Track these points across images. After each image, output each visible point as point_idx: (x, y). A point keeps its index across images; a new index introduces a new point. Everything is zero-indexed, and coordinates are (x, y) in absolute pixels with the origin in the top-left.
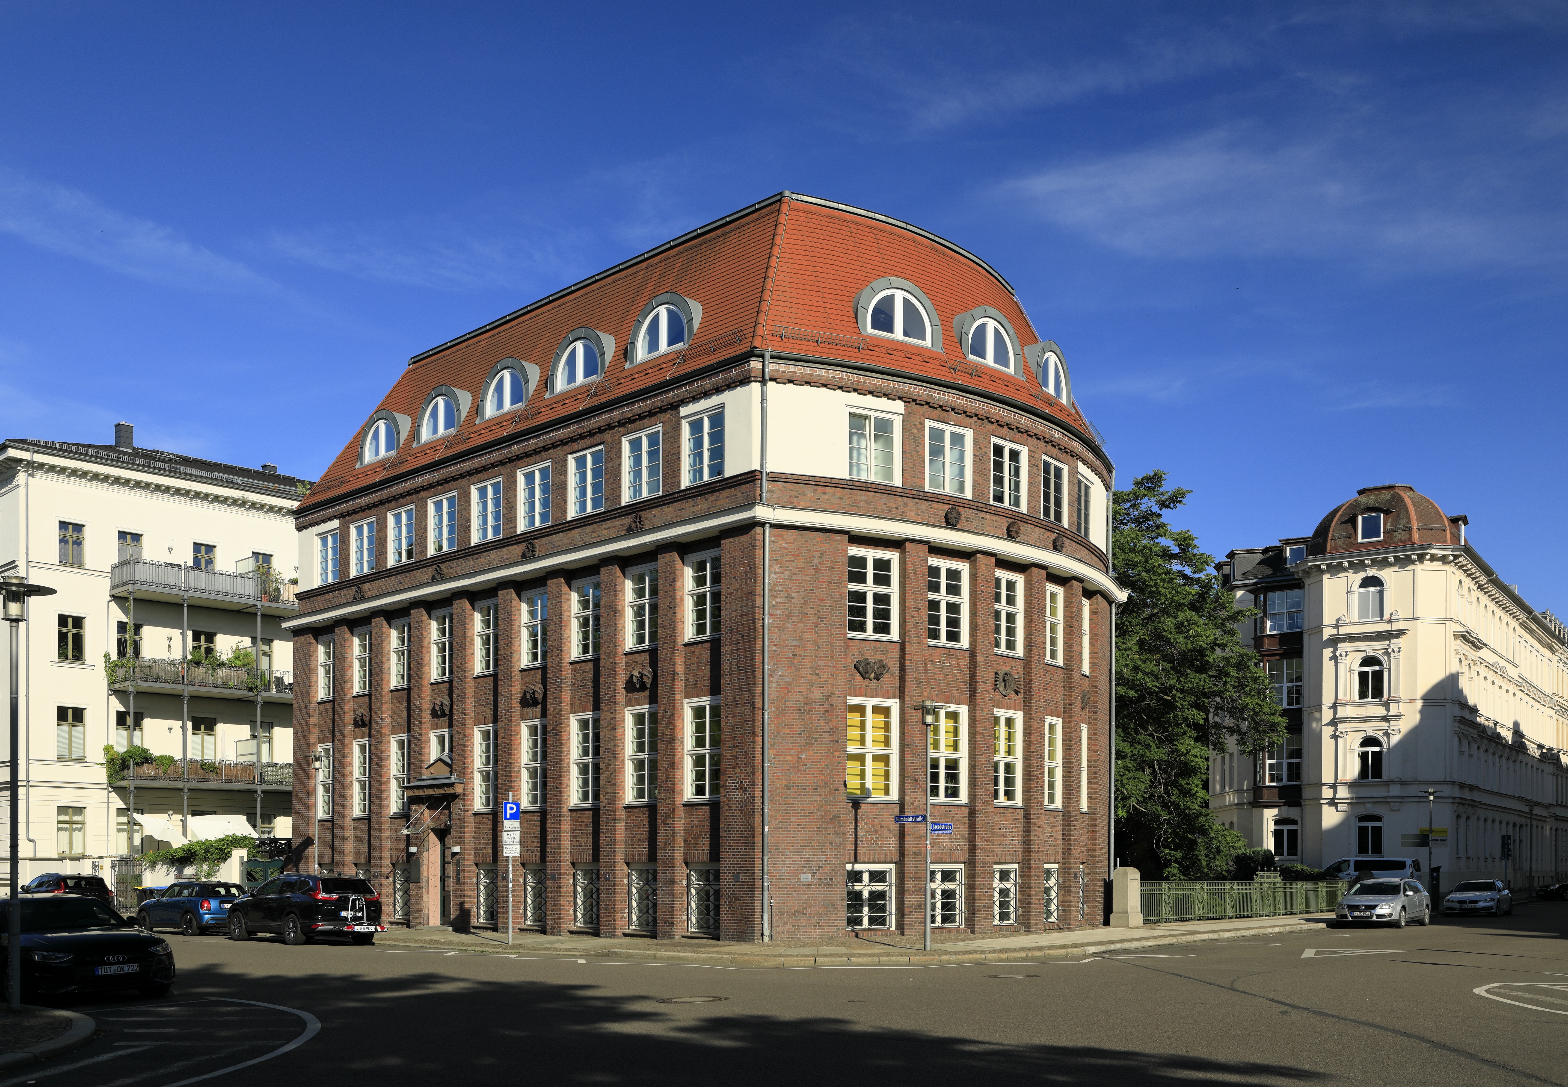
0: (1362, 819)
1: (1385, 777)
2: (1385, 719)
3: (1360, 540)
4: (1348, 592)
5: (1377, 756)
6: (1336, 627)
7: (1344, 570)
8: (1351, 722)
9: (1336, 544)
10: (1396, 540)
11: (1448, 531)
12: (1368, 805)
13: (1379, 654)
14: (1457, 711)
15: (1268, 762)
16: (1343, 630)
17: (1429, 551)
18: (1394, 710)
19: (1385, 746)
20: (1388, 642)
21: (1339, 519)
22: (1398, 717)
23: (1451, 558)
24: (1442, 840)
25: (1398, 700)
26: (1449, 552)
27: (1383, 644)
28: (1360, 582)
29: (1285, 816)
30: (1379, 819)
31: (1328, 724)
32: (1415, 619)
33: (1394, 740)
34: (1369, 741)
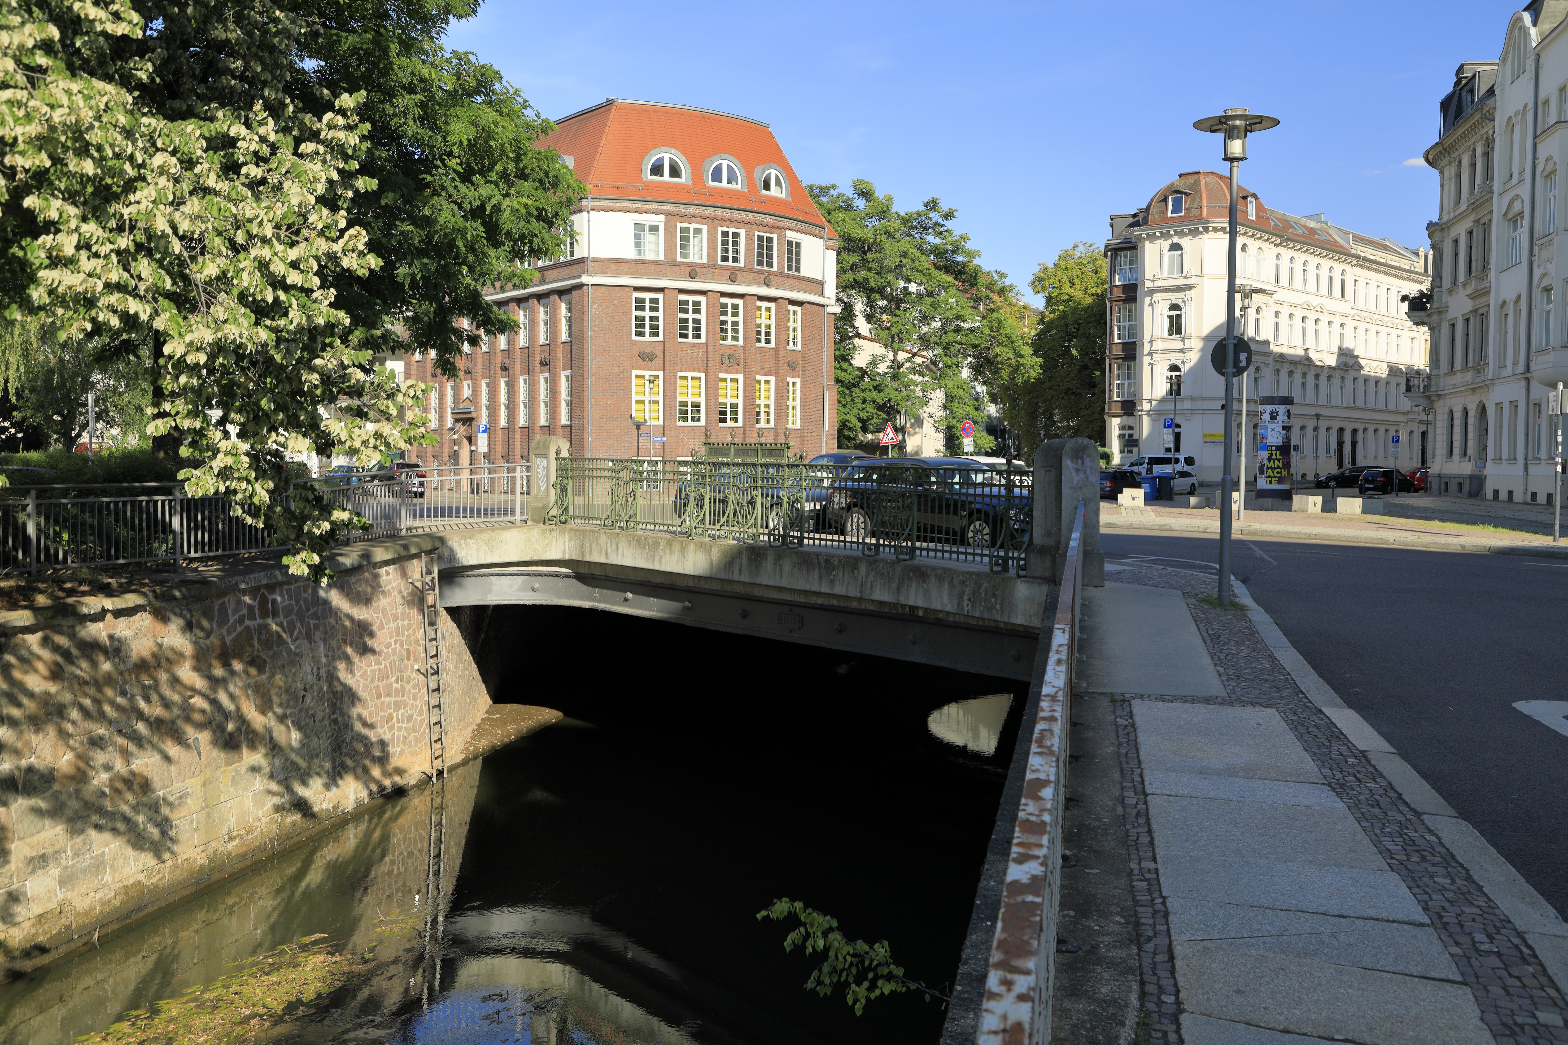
2: (1182, 351)
3: (1170, 215)
6: (1153, 281)
7: (1158, 238)
13: (1179, 302)
15: (1117, 382)
16: (1158, 284)
22: (1190, 349)
25: (1190, 337)
27: (1181, 295)
29: (1125, 423)
32: (1202, 275)
33: (1188, 367)
34: (1174, 368)
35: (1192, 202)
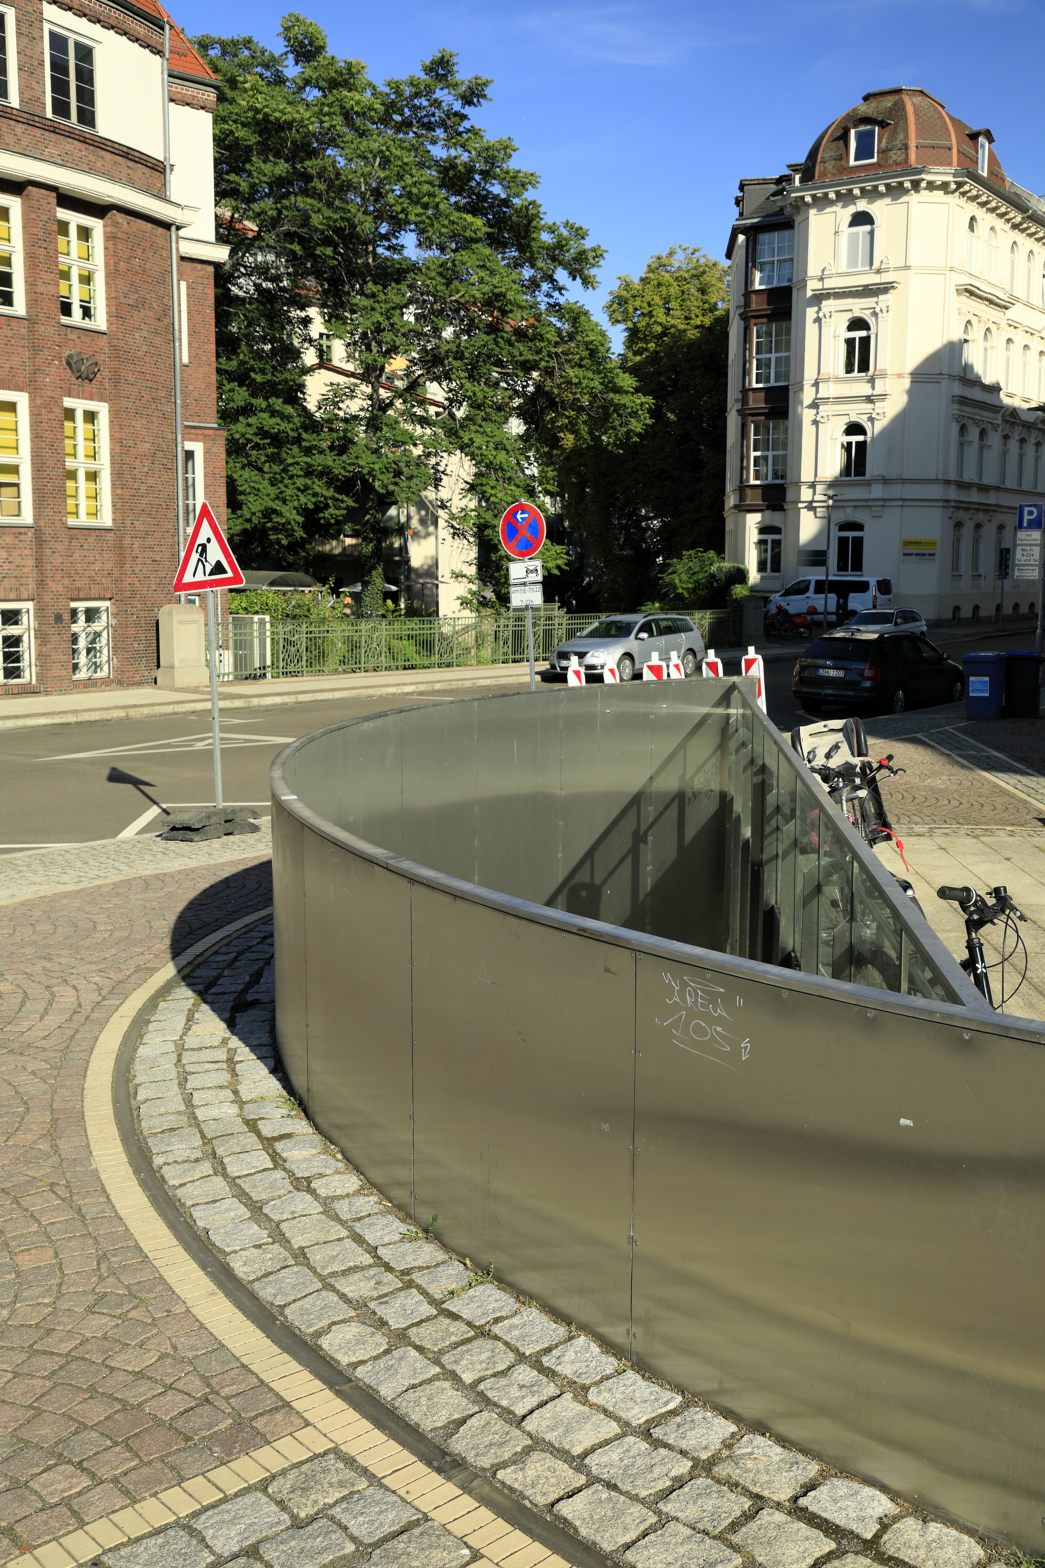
0: (843, 527)
1: (868, 476)
2: (869, 399)
3: (852, 162)
4: (836, 233)
5: (861, 446)
6: (821, 279)
7: (832, 203)
8: (833, 403)
9: (825, 168)
10: (890, 161)
11: (955, 150)
12: (849, 510)
13: (866, 315)
14: (957, 389)
15: (753, 454)
16: (829, 283)
17: (923, 176)
18: (880, 387)
19: (869, 434)
20: (875, 299)
21: (832, 134)
22: (883, 396)
23: (953, 186)
24: (930, 555)
25: (884, 375)
26: (950, 178)
27: (869, 302)
28: (850, 219)
29: (768, 523)
30: (859, 527)
31: (809, 407)
32: (907, 268)
33: (879, 426)
34: (854, 428)
35: (892, 138)
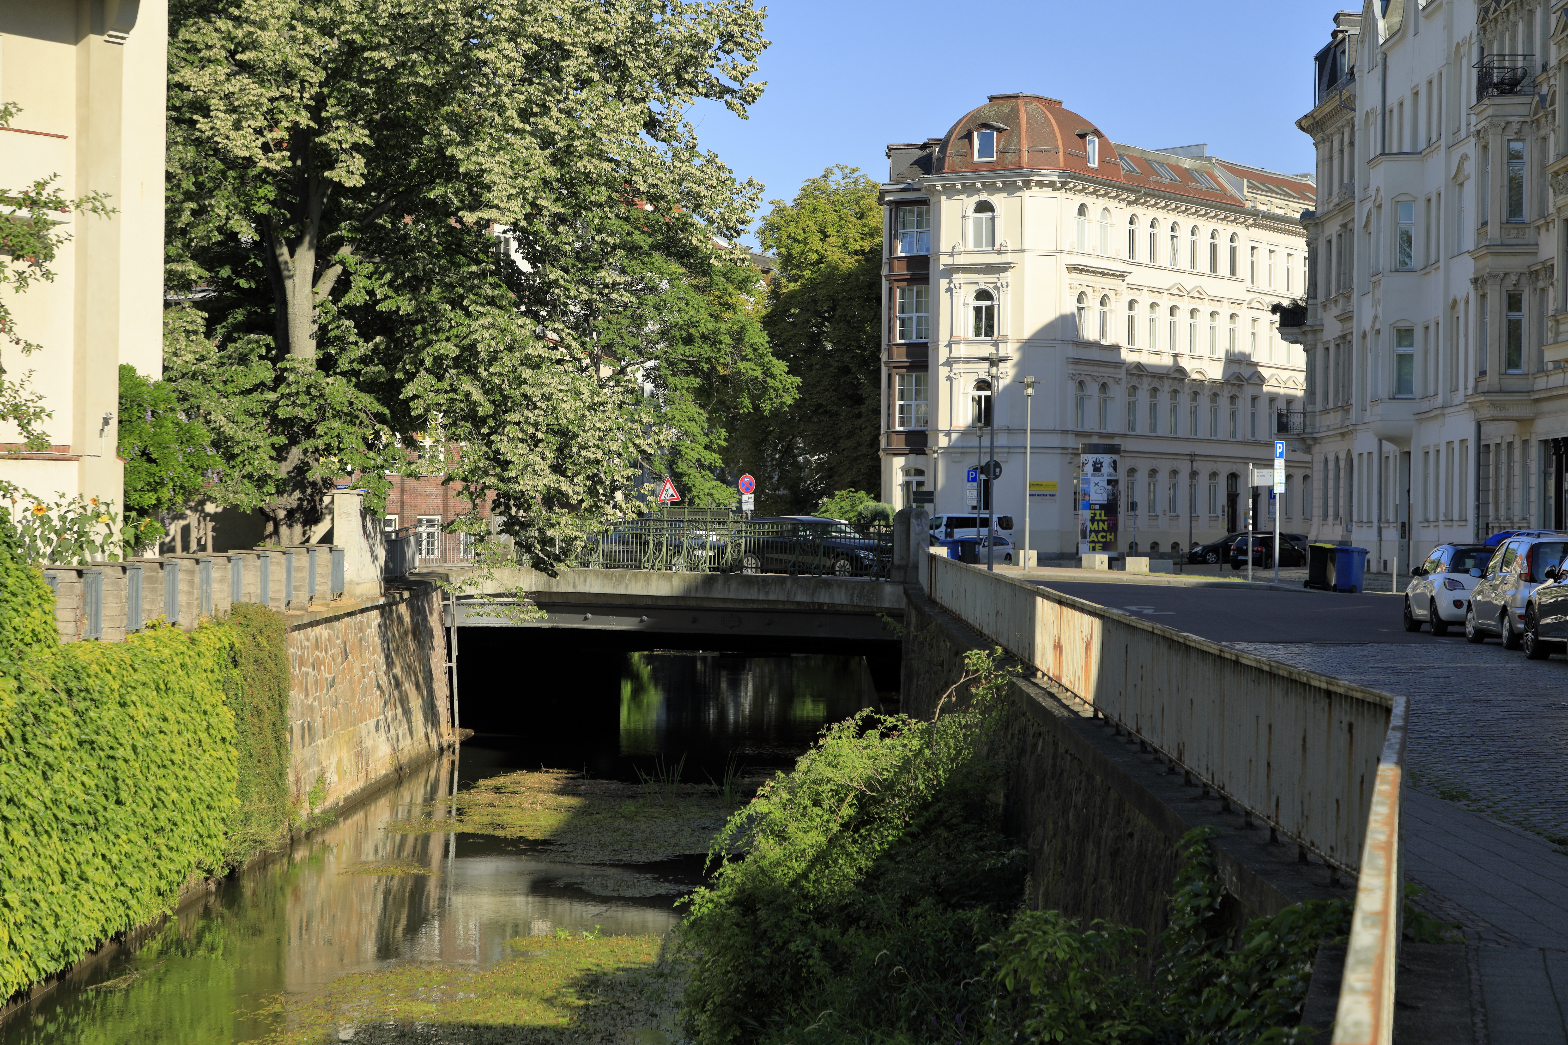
3: (976, 158)
6: (952, 255)
7: (959, 192)
13: (990, 288)
15: (899, 403)
25: (1005, 340)
26: (1056, 179)
27: (992, 277)
31: (944, 364)
32: (1022, 251)
35: (1008, 142)
